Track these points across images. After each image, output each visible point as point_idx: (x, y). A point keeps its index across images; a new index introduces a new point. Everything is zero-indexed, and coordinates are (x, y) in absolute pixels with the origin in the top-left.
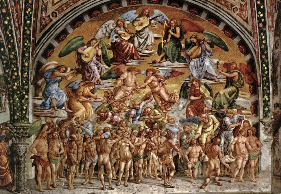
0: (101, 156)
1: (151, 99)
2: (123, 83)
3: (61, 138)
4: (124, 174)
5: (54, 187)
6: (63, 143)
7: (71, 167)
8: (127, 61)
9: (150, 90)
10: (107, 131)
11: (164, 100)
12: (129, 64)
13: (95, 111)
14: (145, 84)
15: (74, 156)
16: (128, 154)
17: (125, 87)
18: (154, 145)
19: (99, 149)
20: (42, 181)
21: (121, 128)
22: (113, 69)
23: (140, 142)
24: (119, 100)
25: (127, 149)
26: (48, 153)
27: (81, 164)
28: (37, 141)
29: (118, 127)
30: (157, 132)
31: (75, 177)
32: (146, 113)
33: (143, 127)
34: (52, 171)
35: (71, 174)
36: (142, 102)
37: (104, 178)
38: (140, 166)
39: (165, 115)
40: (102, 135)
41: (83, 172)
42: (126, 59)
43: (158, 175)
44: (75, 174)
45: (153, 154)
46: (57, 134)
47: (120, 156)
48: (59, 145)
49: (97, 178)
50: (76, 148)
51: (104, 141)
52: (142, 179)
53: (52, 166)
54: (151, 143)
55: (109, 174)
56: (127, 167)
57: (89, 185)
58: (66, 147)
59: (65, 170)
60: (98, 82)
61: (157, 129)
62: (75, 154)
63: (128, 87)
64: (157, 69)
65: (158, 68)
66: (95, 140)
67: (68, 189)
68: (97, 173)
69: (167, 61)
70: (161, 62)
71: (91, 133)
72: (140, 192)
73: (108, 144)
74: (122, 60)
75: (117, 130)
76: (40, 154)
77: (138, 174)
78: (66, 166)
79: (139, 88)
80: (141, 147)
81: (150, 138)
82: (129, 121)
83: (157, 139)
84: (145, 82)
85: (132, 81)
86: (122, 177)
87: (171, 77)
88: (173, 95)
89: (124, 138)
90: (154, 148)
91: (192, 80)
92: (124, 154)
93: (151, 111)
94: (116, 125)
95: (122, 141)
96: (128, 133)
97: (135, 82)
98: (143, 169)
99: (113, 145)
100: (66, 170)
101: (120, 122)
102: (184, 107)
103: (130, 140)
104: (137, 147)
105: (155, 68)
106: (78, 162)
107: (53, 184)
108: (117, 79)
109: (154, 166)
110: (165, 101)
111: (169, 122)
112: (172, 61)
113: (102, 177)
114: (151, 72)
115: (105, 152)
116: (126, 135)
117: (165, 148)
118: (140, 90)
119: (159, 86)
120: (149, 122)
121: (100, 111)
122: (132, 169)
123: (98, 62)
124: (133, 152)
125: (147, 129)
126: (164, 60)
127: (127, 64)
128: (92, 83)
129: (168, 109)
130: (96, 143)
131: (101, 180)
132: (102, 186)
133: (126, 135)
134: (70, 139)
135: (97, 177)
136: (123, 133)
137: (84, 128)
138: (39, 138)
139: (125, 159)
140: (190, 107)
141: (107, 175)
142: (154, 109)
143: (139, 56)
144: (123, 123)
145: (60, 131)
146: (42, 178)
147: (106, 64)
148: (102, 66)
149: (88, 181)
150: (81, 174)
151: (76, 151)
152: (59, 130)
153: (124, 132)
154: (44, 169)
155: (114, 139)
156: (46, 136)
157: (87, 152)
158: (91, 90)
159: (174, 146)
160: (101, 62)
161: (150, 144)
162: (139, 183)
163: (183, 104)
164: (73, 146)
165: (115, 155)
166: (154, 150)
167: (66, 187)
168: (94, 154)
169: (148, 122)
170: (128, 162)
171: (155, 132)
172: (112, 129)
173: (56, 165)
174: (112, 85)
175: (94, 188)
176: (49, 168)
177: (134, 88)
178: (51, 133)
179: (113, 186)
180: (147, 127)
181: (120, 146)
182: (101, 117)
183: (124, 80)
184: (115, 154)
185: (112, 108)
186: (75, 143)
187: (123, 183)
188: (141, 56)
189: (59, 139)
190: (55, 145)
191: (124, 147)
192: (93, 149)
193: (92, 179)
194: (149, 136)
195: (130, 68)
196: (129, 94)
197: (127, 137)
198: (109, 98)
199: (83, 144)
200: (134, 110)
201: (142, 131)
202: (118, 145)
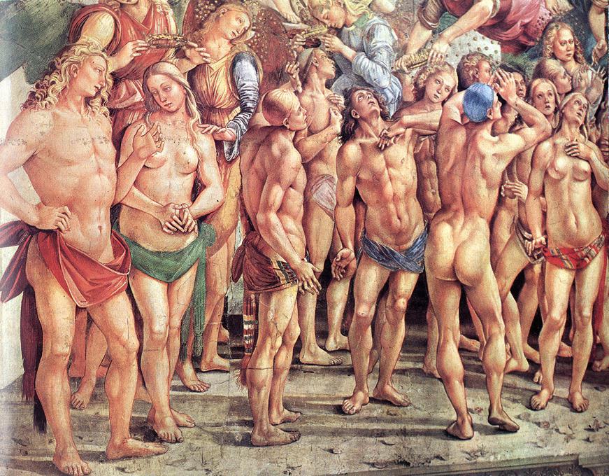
3: (200, 108)
4: (566, 339)
5: (156, 435)
6: (219, 144)
7: (268, 300)
10: (475, 79)
15: (287, 231)
16: (584, 221)
20: (71, 405)
21: (552, 65)
25: (582, 190)
26: (115, 209)
27: (326, 278)
28: (40, 119)
29: (535, 63)
31: (297, 367)
34: (146, 327)
35: (272, 348)
37: (465, 367)
41: (345, 332)
44: (298, 349)
46: (180, 83)
47: (545, 233)
48: (191, 156)
49: (420, 366)
50: (302, 178)
53: (144, 297)
55: (489, 341)
56: (581, 300)
57: (378, 410)
58: (235, 168)
59: (232, 323)
62: (295, 218)
66: (409, 131)
67: (247, 441)
68: (421, 334)
71: (385, 83)
73: (483, 157)
75: (530, 73)
76: (56, 212)
78: (237, 295)
86: (560, 359)
89: (566, 127)
92: (565, 221)
94: (523, 48)
95: (555, 145)
96: (587, 98)
99: (509, 168)
100: (240, 317)
103: (595, 139)
106: (308, 270)
107: (151, 420)
113: (453, 361)
115: (467, 210)
116: (576, 107)
131: (445, 380)
132: (454, 417)
133: (576, 107)
134: (262, 120)
135: (423, 360)
137: (349, 53)
138: (52, 97)
139: (570, 252)
141: (475, 345)
145: (198, 61)
146: (72, 380)
149: (371, 384)
150: (331, 344)
151: (296, 199)
152: (188, 53)
154: (90, 320)
156: (98, 93)
157: (361, 208)
164: (277, 163)
165: (520, 226)
167: (237, 431)
168: (405, 217)
170: (587, 265)
173: (170, 286)
175: (404, 433)
176: (119, 311)
178: (139, 71)
179: (513, 412)
184: (519, 219)
186: (290, 145)
187: (563, 392)
189: (189, 114)
190: (165, 153)
191: (567, 180)
197: (581, 121)
199: (341, 152)
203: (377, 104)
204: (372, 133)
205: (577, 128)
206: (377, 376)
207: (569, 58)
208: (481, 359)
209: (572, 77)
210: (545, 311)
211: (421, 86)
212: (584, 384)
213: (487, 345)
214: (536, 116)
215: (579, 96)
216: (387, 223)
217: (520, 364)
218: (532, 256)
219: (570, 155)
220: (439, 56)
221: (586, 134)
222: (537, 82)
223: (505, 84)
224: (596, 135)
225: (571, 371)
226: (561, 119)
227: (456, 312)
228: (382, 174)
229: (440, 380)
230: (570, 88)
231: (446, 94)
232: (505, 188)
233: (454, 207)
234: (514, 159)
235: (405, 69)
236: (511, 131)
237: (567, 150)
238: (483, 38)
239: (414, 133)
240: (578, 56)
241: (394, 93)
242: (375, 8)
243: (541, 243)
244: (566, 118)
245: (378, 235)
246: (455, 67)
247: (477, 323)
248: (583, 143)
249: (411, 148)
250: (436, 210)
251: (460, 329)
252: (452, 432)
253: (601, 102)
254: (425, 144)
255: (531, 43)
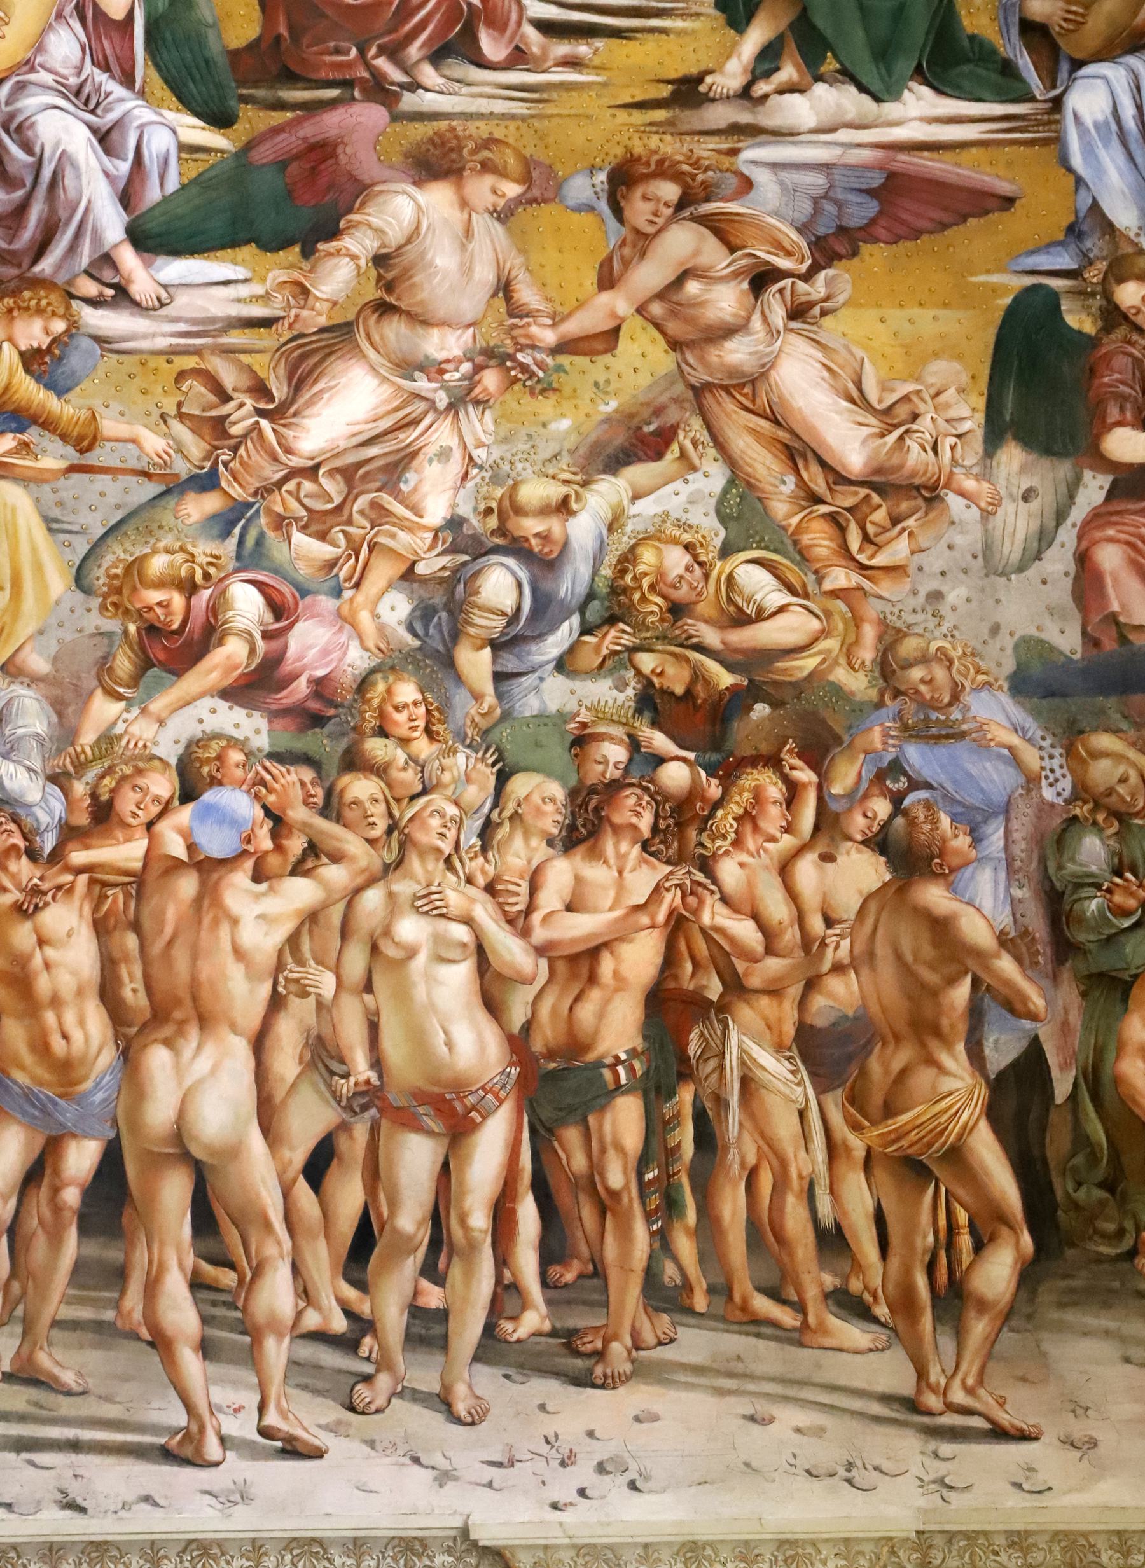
0: (158, 1059)
1: (683, 455)
2: (372, 293)
4: (431, 1271)
8: (407, 72)
9: (663, 360)
10: (215, 782)
11: (823, 463)
12: (428, 101)
13: (80, 568)
14: (606, 297)
17: (394, 330)
18: (760, 949)
19: (139, 985)
21: (377, 748)
22: (264, 154)
23: (595, 910)
24: (338, 463)
29: (344, 744)
30: (775, 791)
32: (644, 599)
33: (612, 739)
36: (585, 484)
37: (206, 1320)
38: (616, 1176)
39: (857, 621)
40: (164, 828)
42: (394, 52)
43: (829, 1281)
45: (749, 1044)
47: (377, 1063)
49: (109, 1315)
51: (187, 885)
52: (649, 1337)
54: (713, 914)
55: (258, 1271)
56: (463, 1193)
57: (18, 1398)
60: (108, 275)
61: (774, 762)
63: (435, 333)
64: (726, 161)
65: (734, 152)
66: (83, 878)
68: (114, 1254)
69: (819, 78)
70: (761, 88)
72: (633, 1486)
73: (235, 922)
74: (349, 65)
75: (332, 766)
77: (598, 1272)
79: (549, 337)
80: (607, 965)
81: (706, 865)
82: (459, 679)
83: (785, 869)
84: (607, 280)
85: (467, 270)
86: (416, 1311)
87: (876, 240)
88: (915, 417)
89: (415, 863)
90: (755, 982)
91: (1103, 265)
92: (418, 1038)
93: (698, 570)
94: (317, 720)
95: (391, 895)
96: (456, 803)
97: (504, 288)
98: (649, 1217)
99: (293, 941)
101: (364, 684)
102: (1044, 539)
103: (481, 881)
104: (561, 967)
105: (706, 148)
108: (308, 252)
109: (780, 1184)
110: (837, 478)
111: (897, 693)
112: (876, 86)
114: (670, 191)
115: (204, 1021)
116: (435, 822)
117: (887, 971)
118: (564, 360)
119: (756, 322)
120: (679, 690)
121: (135, 568)
122: (528, 1213)
123: (101, 77)
124: (518, 1016)
125: (660, 760)
126: (788, 72)
127: (410, 101)
128: (39, 283)
129: (878, 561)
130: (96, 909)
133: (435, 822)
135: (117, 1305)
136: (396, 797)
140: (1111, 540)
141: (228, 1278)
142: (726, 551)
143: (530, 32)
144: (389, 691)
147: (180, 99)
148: (143, 113)
153: (413, 798)
155: (298, 870)
158: (32, 360)
159: (979, 954)
160: (128, 80)
161: (703, 931)
162: (609, 1383)
163: (1035, 505)
166: (764, 1002)
168: (77, 1036)
169: (667, 693)
170: (474, 1127)
171: (758, 796)
172: (276, 756)
174: (258, 311)
177: (495, 338)
180: (660, 741)
181: (375, 949)
182: (152, 630)
183: (380, 260)
185: (260, 541)
187: (427, 1379)
188: (547, 28)
191: (421, 960)
192: (66, 982)
193: (56, 1333)
194: (692, 834)
195: (438, 141)
196: (442, 404)
197: (447, 848)
198: (226, 435)
200: (510, 561)
201: (614, 787)
202: (345, 932)
203: (17, 834)
204: (9, 886)
205: (437, 860)
206: (19, 1330)
207: (416, 734)
208: (240, 1304)
209: (423, 767)
210: (379, 1215)
211: (105, 797)
212: (478, 1367)
213: (252, 1279)
214: (348, 842)
215: (437, 800)
216: (41, 1047)
217: (326, 1319)
218: (349, 1108)
219: (426, 913)
220: (140, 744)
221: (462, 875)
222: (346, 779)
223: (276, 786)
224: (483, 872)
225: (445, 1337)
226: (402, 846)
227: (185, 1214)
228: (29, 957)
229: (151, 1344)
230: (420, 788)
231: (155, 809)
232: (286, 979)
233: (178, 1015)
234: (302, 923)
235: (71, 769)
236: (293, 873)
237: (419, 903)
238: (231, 708)
239: (92, 882)
240: (435, 728)
241: (50, 813)
242: (12, 670)
243: (368, 1082)
244: (414, 844)
245: (21, 1067)
246: (173, 761)
247: (232, 1236)
248: (455, 890)
249: (87, 909)
250: (140, 1021)
251: (194, 1244)
252: (176, 1451)
253: (491, 810)
254: (115, 901)
255: (332, 712)
